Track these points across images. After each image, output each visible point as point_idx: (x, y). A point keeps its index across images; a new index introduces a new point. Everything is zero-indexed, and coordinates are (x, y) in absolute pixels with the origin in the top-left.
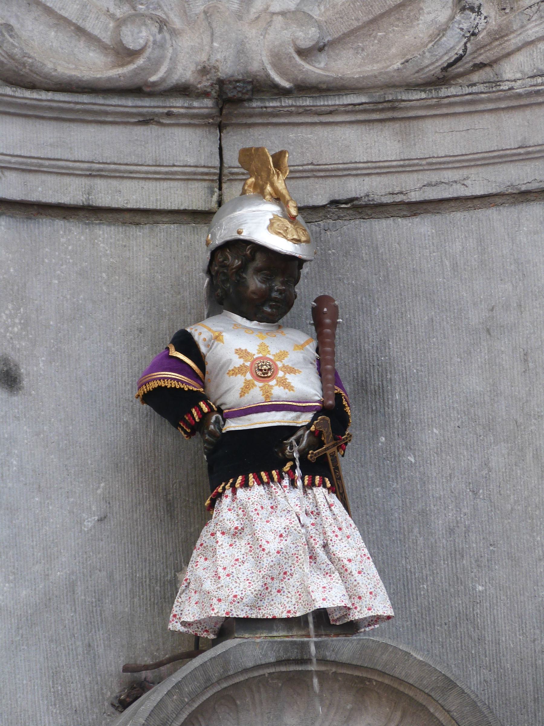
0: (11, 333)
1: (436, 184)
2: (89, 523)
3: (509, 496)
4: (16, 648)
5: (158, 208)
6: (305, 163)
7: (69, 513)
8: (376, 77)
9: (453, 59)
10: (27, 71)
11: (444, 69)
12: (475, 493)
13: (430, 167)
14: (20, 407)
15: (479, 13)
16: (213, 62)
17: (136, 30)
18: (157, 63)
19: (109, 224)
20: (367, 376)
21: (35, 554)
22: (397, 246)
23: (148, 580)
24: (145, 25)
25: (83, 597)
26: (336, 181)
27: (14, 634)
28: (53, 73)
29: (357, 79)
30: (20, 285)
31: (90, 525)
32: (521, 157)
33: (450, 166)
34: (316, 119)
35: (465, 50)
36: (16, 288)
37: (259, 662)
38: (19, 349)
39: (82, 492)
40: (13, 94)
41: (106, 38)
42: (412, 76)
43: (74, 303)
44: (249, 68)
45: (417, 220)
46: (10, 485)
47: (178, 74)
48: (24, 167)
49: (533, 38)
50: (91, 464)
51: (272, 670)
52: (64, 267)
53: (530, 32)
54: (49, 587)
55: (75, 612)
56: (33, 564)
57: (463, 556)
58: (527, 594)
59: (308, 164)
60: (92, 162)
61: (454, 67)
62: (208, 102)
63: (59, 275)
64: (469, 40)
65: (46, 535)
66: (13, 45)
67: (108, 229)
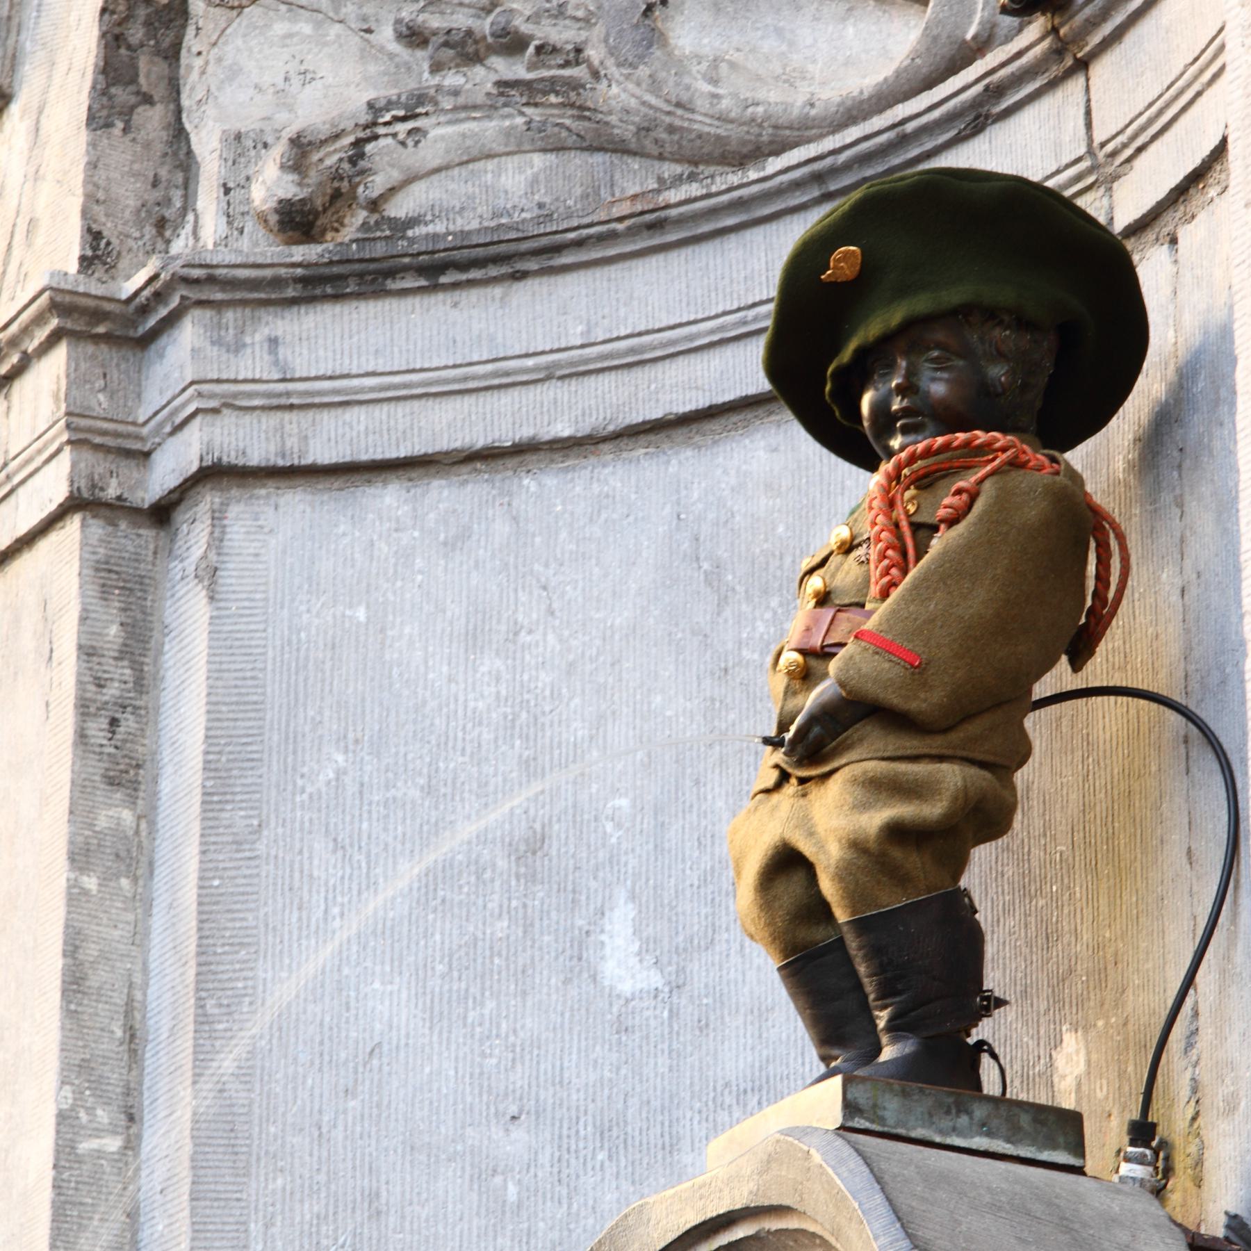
10: (770, 131)
28: (813, 112)
40: (704, 191)
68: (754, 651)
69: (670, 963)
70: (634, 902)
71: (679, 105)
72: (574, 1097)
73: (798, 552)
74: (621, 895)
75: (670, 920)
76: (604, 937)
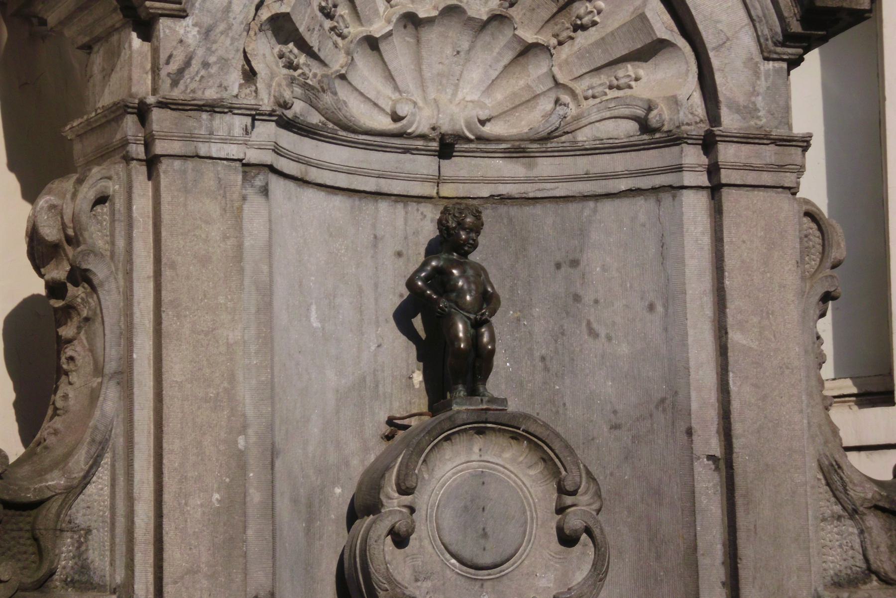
11: (549, 134)
12: (556, 341)
18: (411, 124)
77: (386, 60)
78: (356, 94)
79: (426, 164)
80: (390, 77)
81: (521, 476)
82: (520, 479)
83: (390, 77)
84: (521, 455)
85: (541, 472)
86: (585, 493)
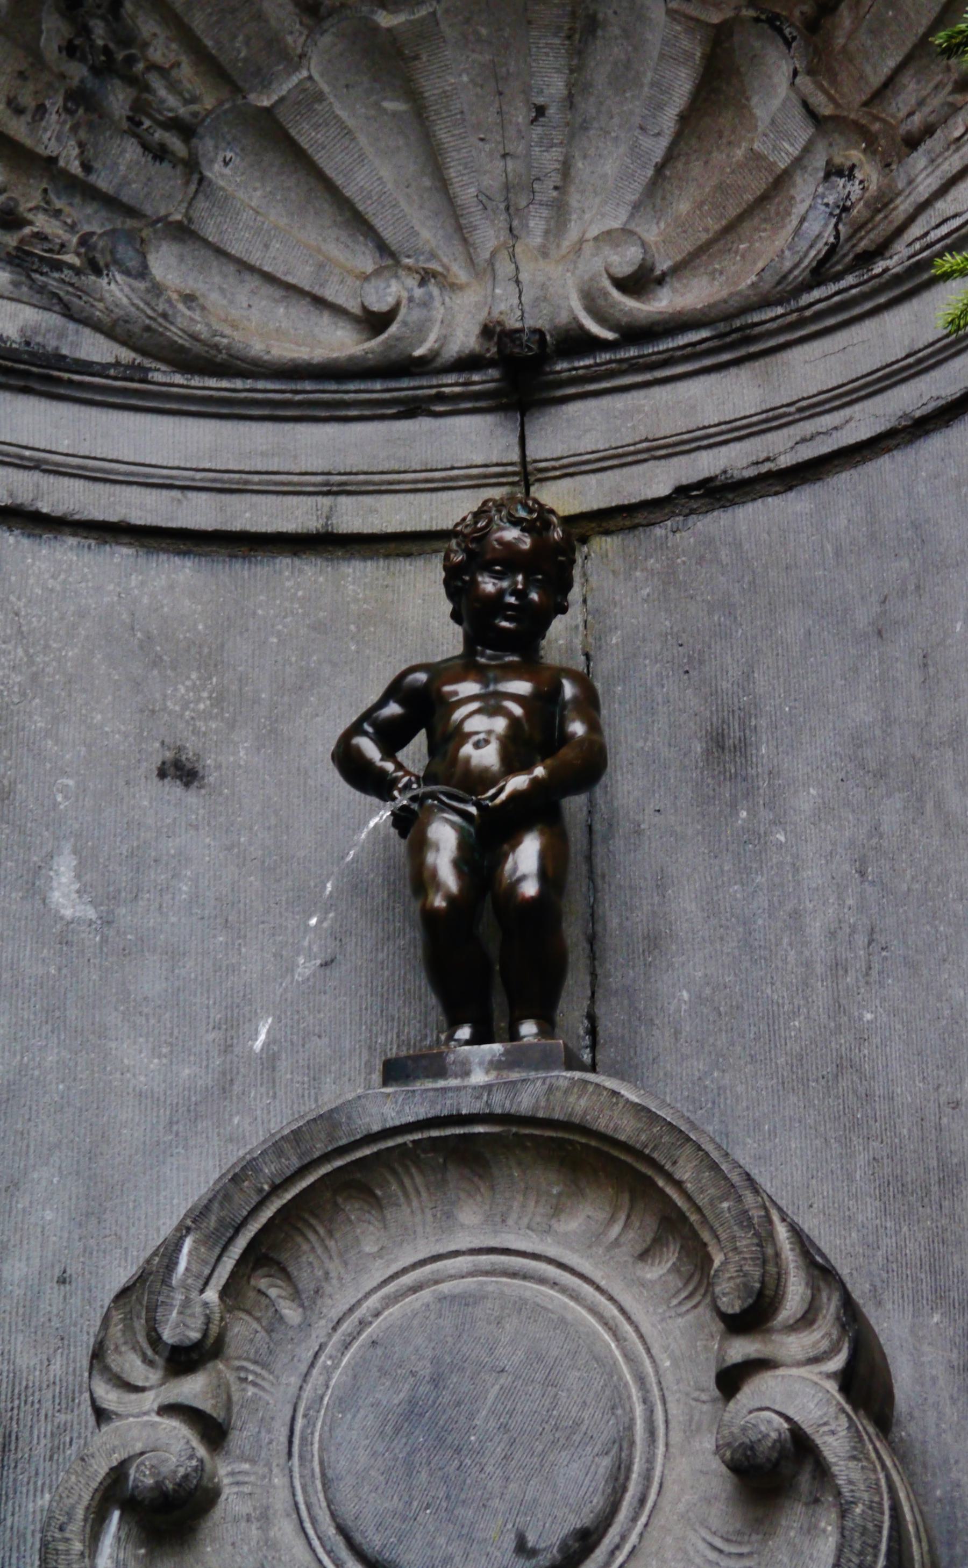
0: (193, 710)
1: (812, 438)
2: (305, 967)
3: (904, 871)
4: (164, 1152)
5: (434, 528)
6: (637, 439)
7: (275, 955)
8: (725, 301)
9: (823, 252)
10: (225, 357)
12: (862, 874)
13: (803, 415)
14: (201, 811)
15: (851, 177)
16: (495, 314)
17: (382, 285)
18: (421, 331)
19: (364, 558)
20: (725, 726)
21: (212, 1016)
22: (766, 535)
23: (395, 1047)
24: (397, 276)
25: (289, 1076)
26: (683, 459)
27: (162, 1131)
28: (266, 357)
29: (701, 310)
30: (214, 646)
31: (307, 972)
32: (912, 371)
33: (827, 406)
34: (648, 377)
35: (837, 237)
36: (206, 650)
37: (389, 1124)
38: (205, 734)
39: (298, 927)
40: (185, 383)
41: (353, 306)
42: (774, 291)
43: (301, 668)
44: (557, 321)
45: (791, 495)
46: (173, 919)
47: (459, 342)
48: (219, 485)
49: (927, 195)
50: (315, 886)
51: (417, 1136)
52: (288, 620)
53: (921, 188)
54: (231, 1062)
55: (274, 1097)
56: (207, 1031)
57: (846, 971)
58: (928, 1016)
59: (641, 442)
60: (329, 473)
61: (828, 265)
62: (493, 373)
63: (279, 631)
64: (839, 219)
65: (232, 988)
66: (192, 319)
67: (362, 564)
68: (175, 704)
69: (101, 905)
70: (75, 853)
71: (164, 316)
72: (27, 981)
73: (214, 646)
74: (67, 847)
75: (103, 875)
76: (52, 873)
77: (330, 172)
78: (253, 282)
79: (475, 440)
80: (357, 222)
81: (616, 1289)
82: (611, 1299)
83: (357, 222)
84: (612, 1220)
85: (675, 1269)
86: (807, 1320)
